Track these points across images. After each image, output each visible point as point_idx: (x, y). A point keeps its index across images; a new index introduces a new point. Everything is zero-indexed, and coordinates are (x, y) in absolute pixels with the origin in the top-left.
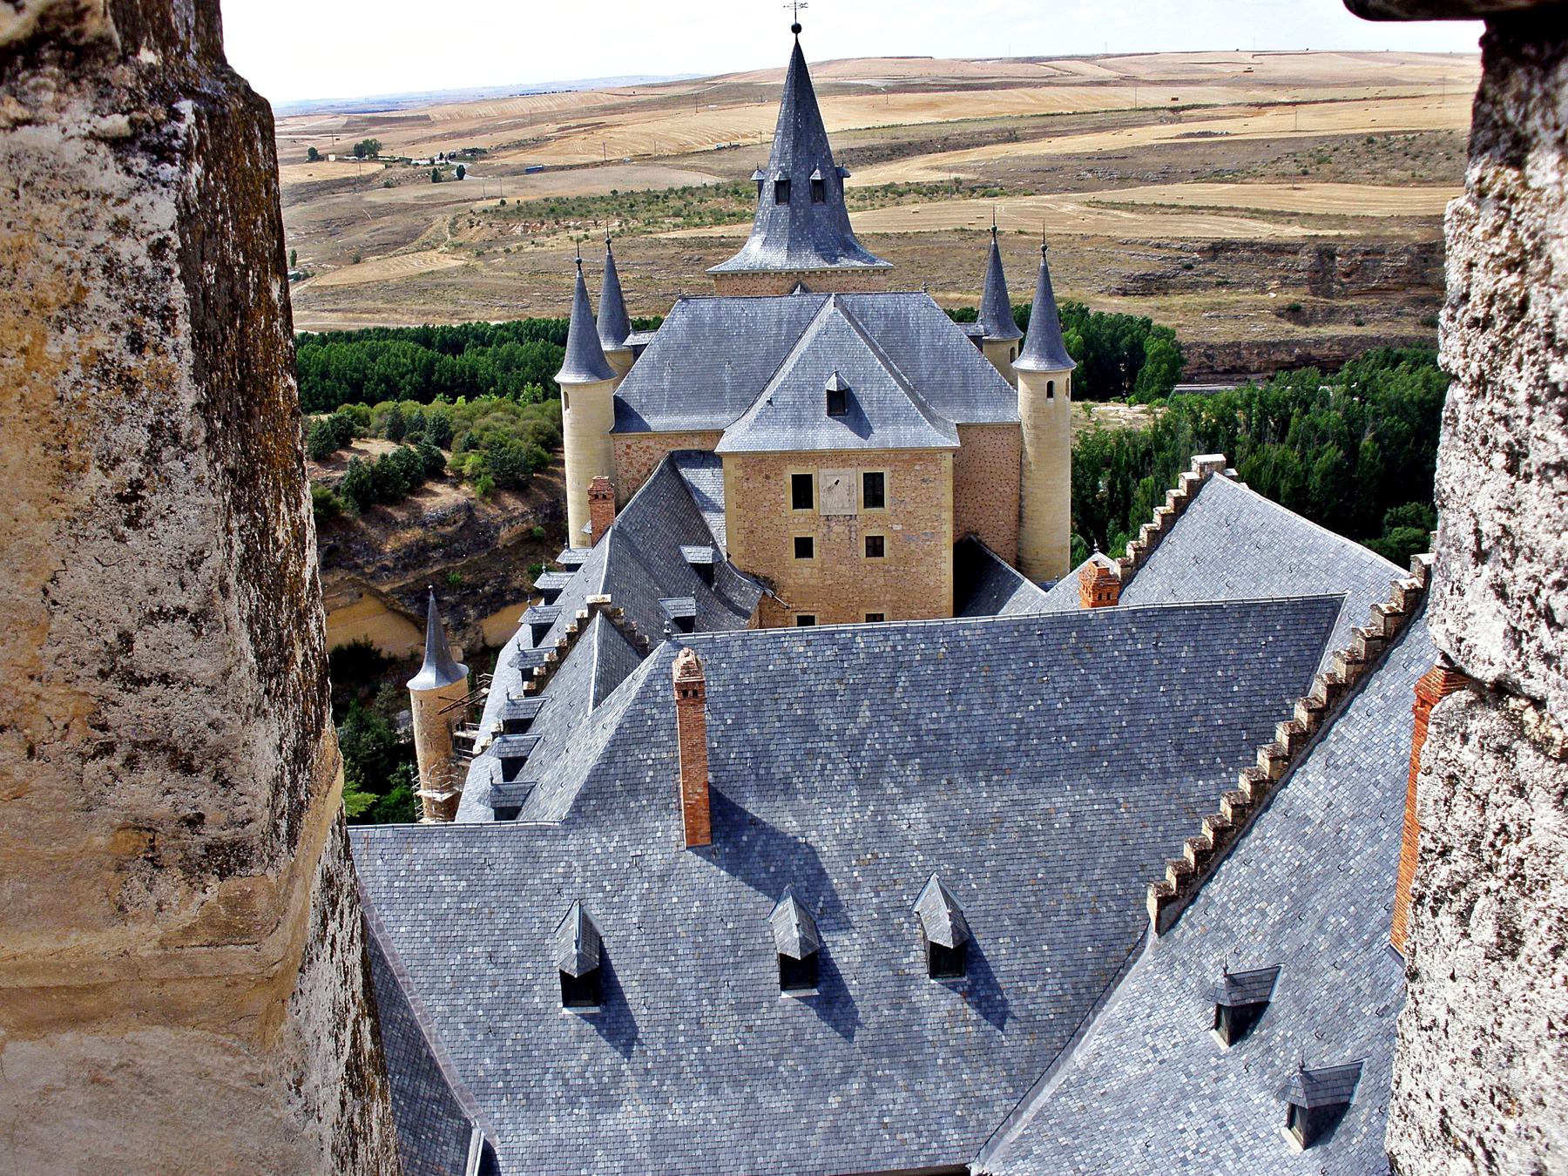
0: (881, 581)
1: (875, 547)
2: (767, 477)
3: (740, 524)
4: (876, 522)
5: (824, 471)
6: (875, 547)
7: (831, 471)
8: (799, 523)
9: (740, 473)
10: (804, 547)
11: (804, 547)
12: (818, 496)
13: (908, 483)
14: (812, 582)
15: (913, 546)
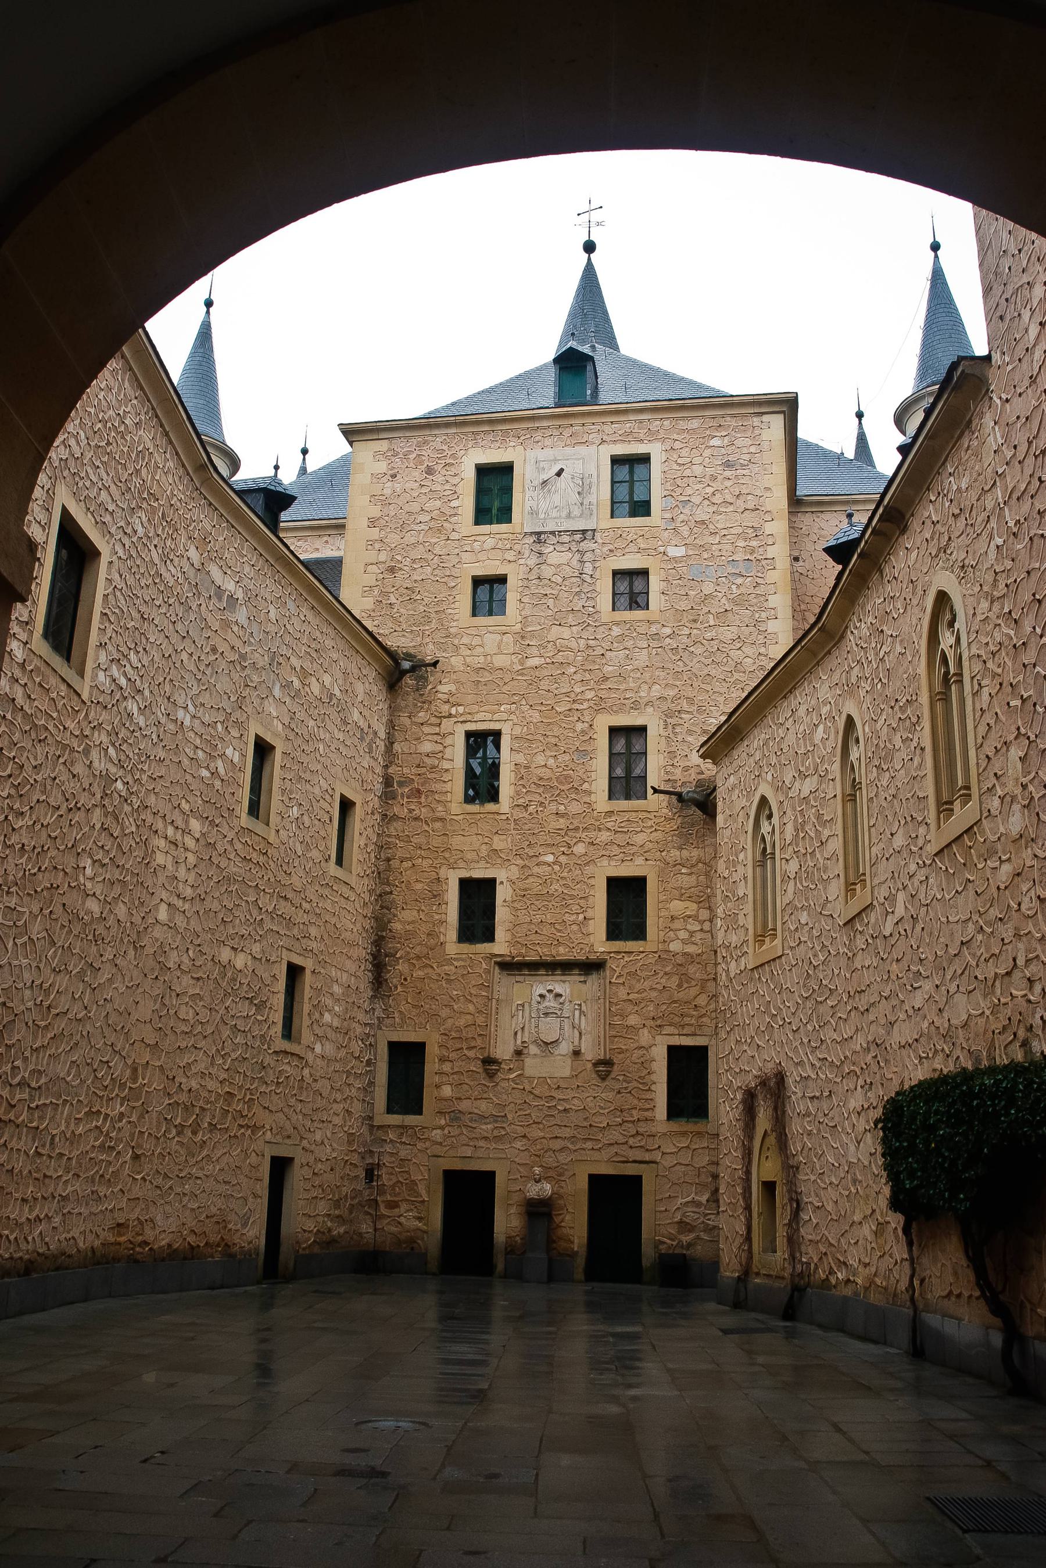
0: (642, 658)
1: (631, 587)
2: (430, 471)
3: (372, 556)
4: (629, 544)
5: (536, 453)
6: (631, 587)
7: (548, 453)
8: (487, 550)
9: (382, 467)
10: (488, 590)
11: (488, 590)
12: (522, 499)
13: (698, 470)
14: (499, 661)
15: (708, 588)
